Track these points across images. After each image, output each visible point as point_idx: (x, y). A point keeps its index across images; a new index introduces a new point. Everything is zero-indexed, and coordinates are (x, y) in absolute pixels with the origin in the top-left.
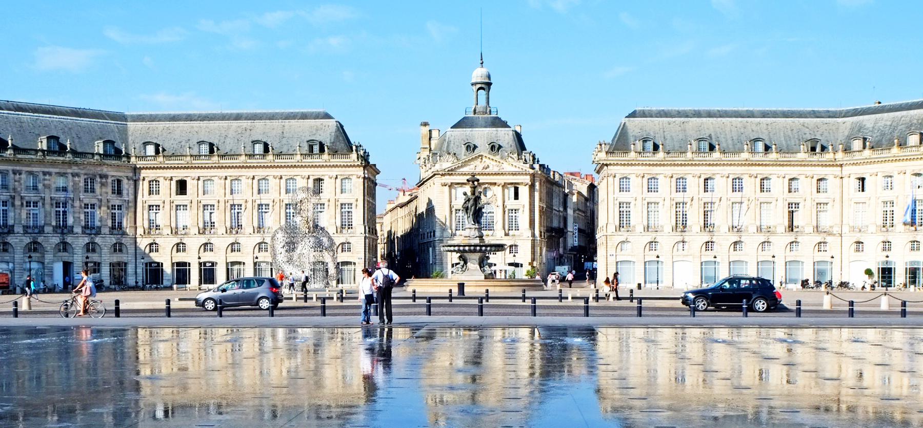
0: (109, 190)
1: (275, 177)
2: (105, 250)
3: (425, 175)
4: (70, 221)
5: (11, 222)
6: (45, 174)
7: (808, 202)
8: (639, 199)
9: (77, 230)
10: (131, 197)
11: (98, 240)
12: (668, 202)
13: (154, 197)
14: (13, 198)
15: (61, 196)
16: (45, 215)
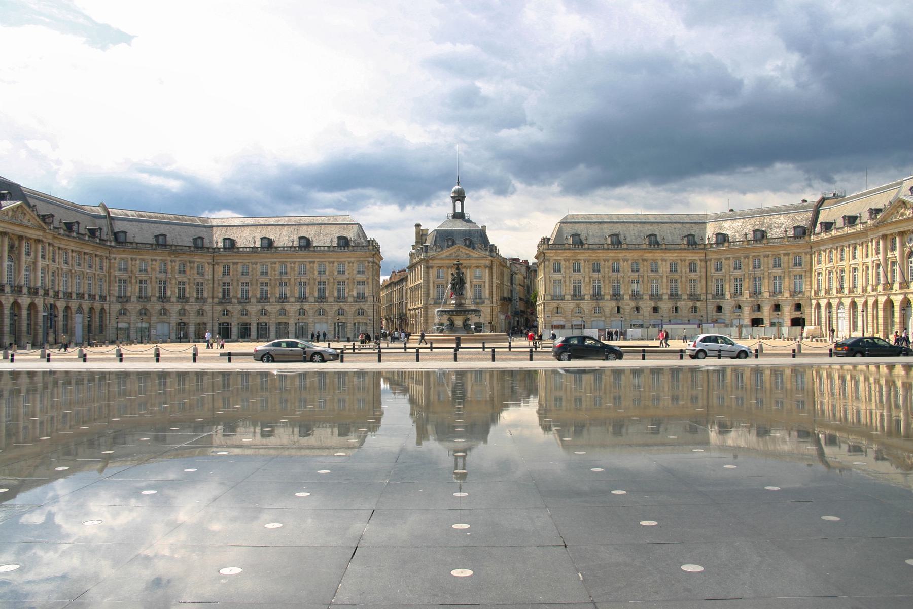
0: (195, 272)
1: (310, 262)
2: (192, 314)
3: (415, 261)
4: (169, 293)
5: (129, 294)
6: (152, 260)
7: (684, 279)
8: (567, 276)
9: (174, 299)
10: (211, 276)
11: (187, 307)
12: (587, 280)
13: (227, 277)
14: (131, 277)
15: (163, 276)
16: (153, 290)
